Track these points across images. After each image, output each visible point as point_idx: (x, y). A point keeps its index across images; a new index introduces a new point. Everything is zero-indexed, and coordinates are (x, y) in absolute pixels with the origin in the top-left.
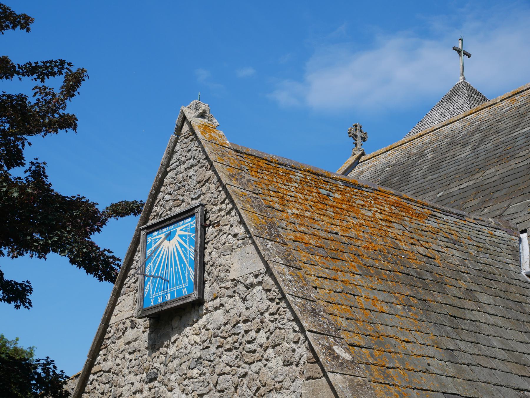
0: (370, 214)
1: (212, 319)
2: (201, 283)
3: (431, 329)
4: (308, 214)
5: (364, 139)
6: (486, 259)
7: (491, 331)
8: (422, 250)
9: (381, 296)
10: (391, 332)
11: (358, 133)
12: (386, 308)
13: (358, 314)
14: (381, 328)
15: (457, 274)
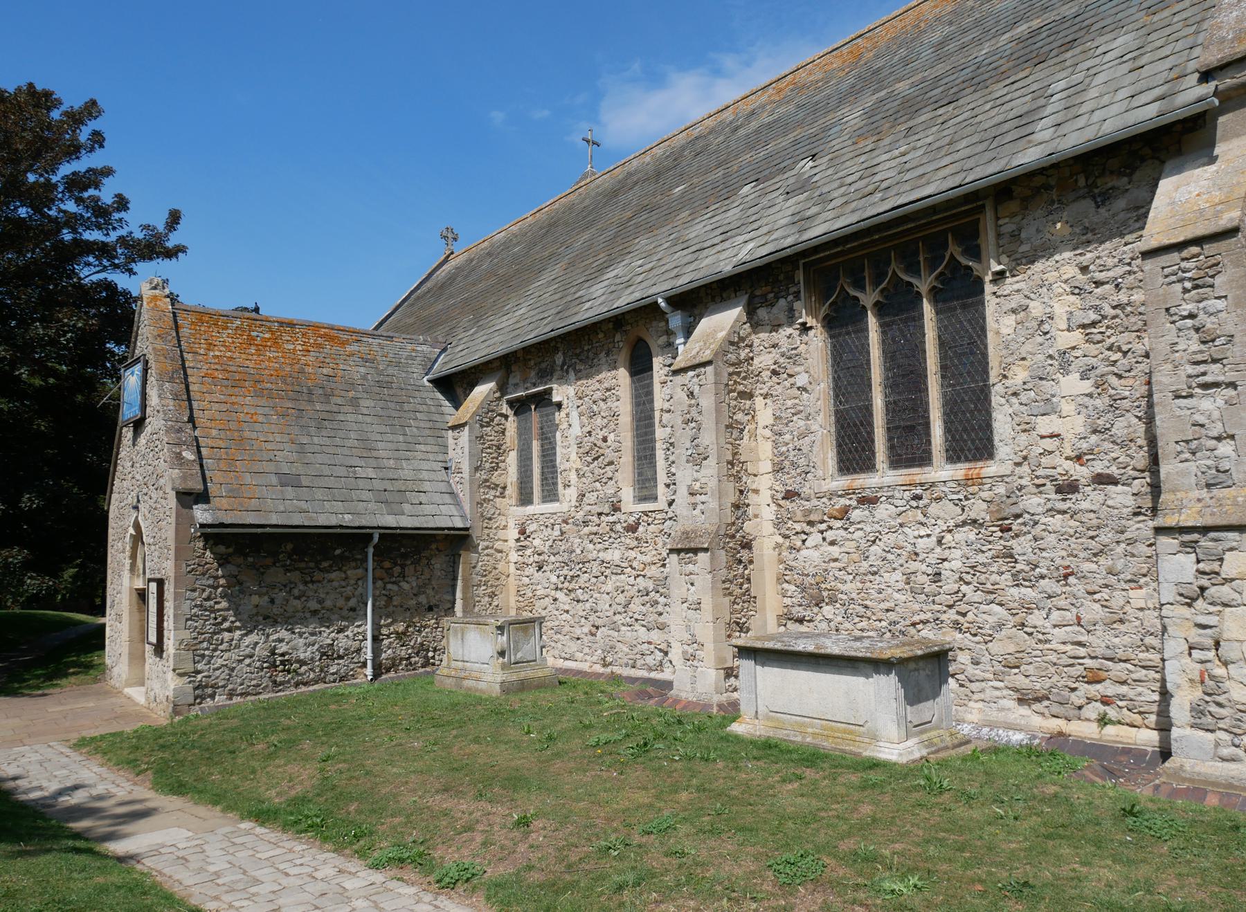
0: (292, 347)
1: (148, 429)
2: (144, 406)
3: (296, 430)
4: (229, 354)
5: (455, 239)
6: (390, 371)
7: (355, 427)
8: (325, 371)
9: (260, 410)
10: (254, 436)
11: (450, 235)
12: (261, 419)
13: (232, 425)
14: (247, 434)
15: (352, 385)
